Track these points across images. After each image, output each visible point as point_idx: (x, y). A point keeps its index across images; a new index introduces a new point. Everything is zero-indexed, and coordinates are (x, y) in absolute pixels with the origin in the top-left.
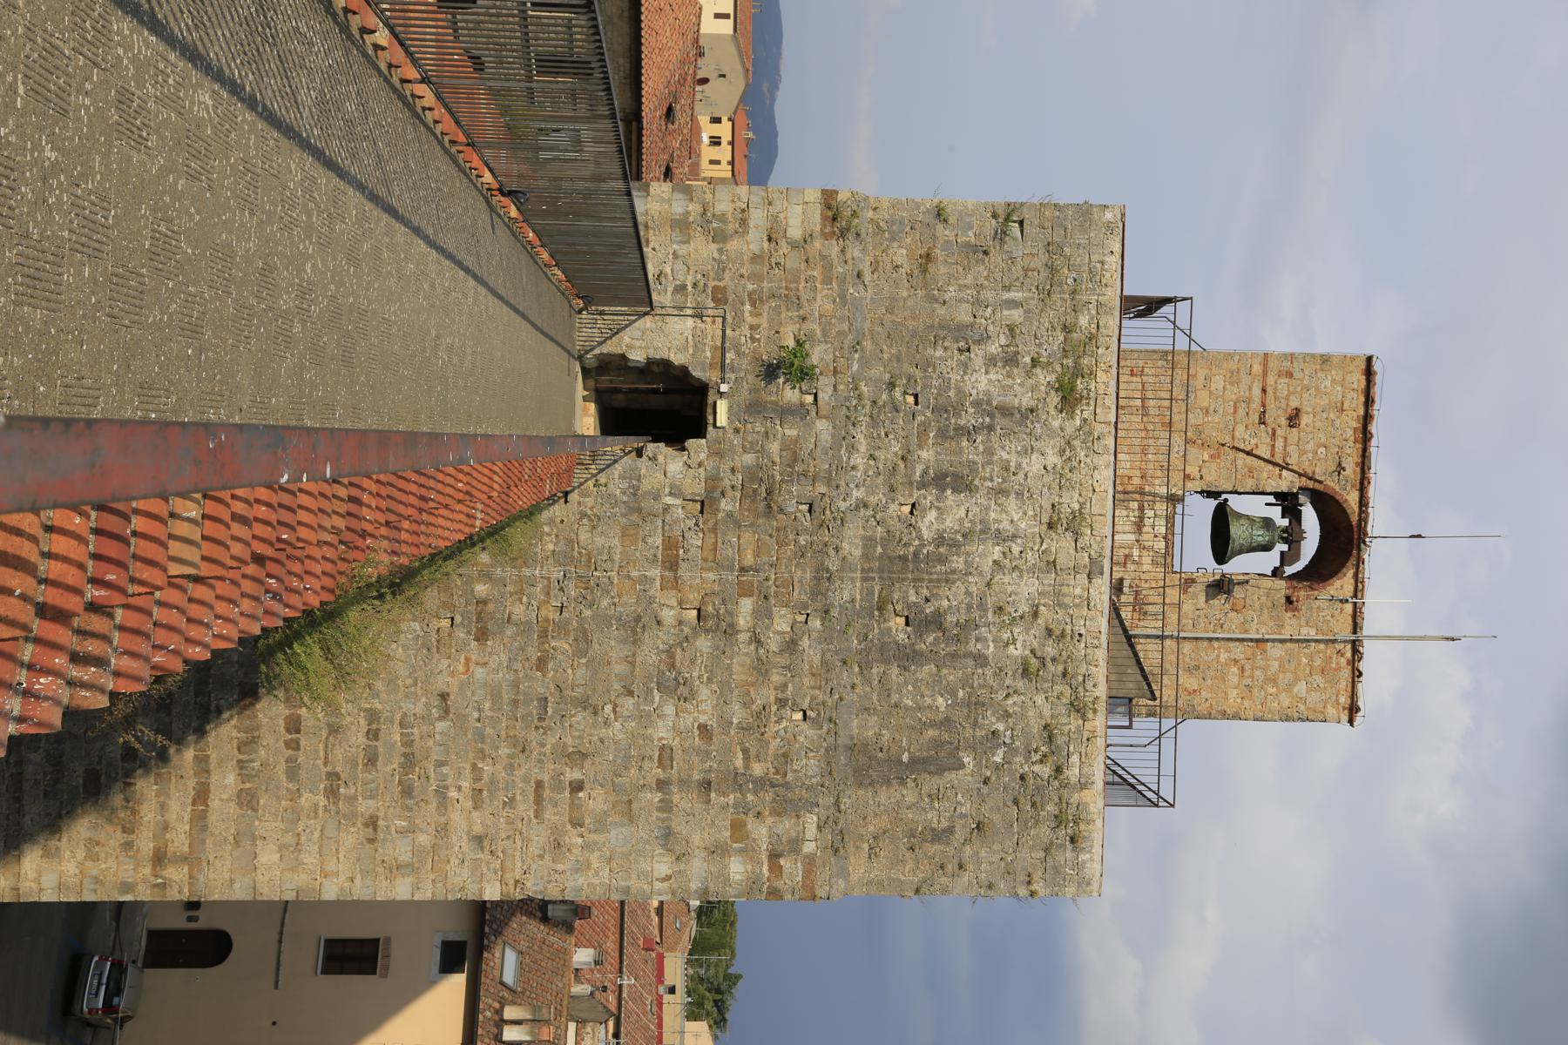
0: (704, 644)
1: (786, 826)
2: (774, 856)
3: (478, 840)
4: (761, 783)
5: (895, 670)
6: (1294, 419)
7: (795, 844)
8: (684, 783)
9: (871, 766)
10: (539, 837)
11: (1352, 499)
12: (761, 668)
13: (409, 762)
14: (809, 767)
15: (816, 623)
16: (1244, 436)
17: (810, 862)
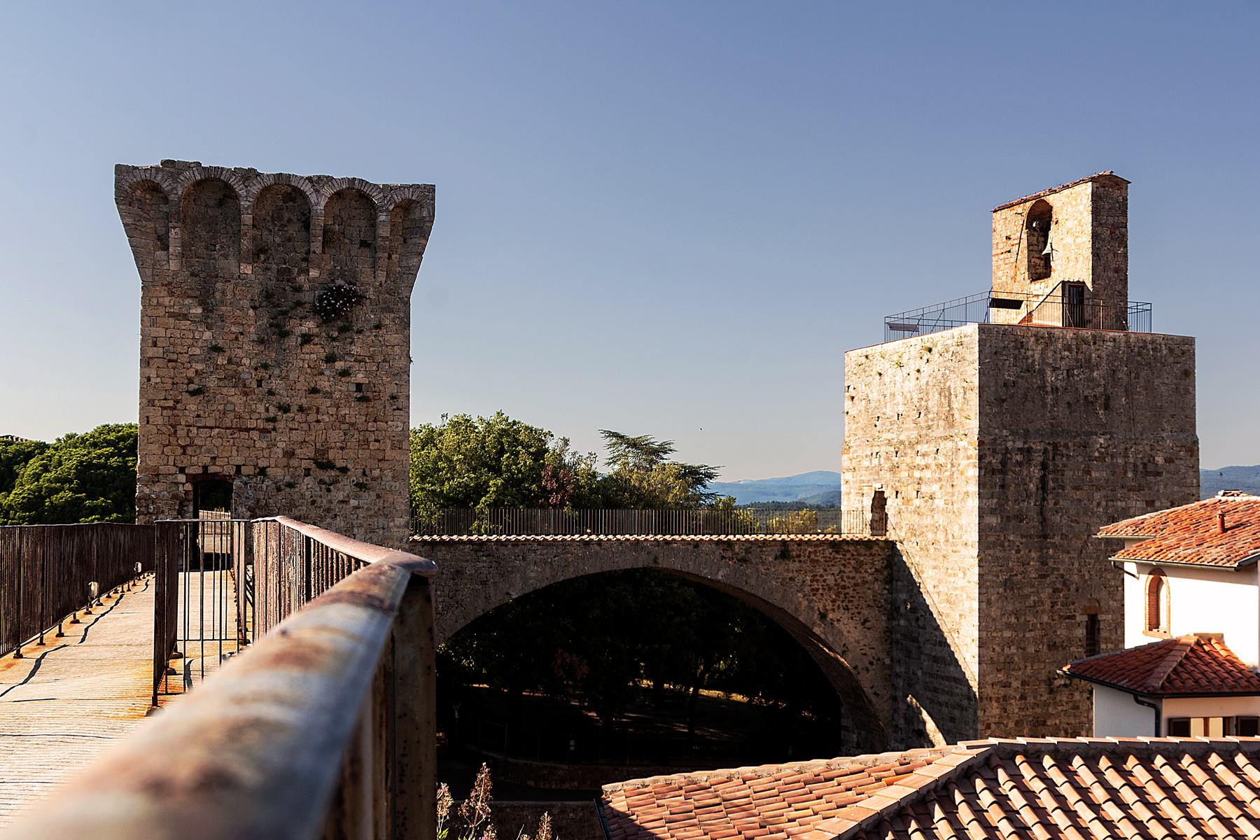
0: (924, 489)
1: (961, 454)
2: (969, 458)
3: (965, 574)
4: (953, 465)
5: (930, 416)
6: (1008, 238)
7: (966, 449)
8: (953, 495)
9: (950, 420)
10: (964, 551)
11: (1029, 204)
12: (927, 467)
13: (948, 601)
14: (949, 444)
15: (919, 447)
16: (1013, 260)
17: (969, 443)
